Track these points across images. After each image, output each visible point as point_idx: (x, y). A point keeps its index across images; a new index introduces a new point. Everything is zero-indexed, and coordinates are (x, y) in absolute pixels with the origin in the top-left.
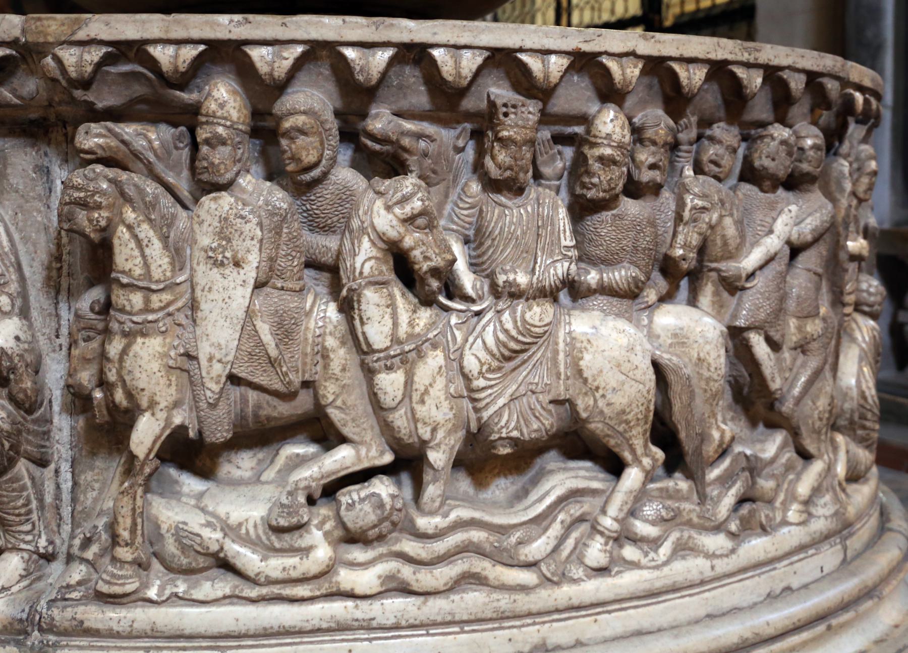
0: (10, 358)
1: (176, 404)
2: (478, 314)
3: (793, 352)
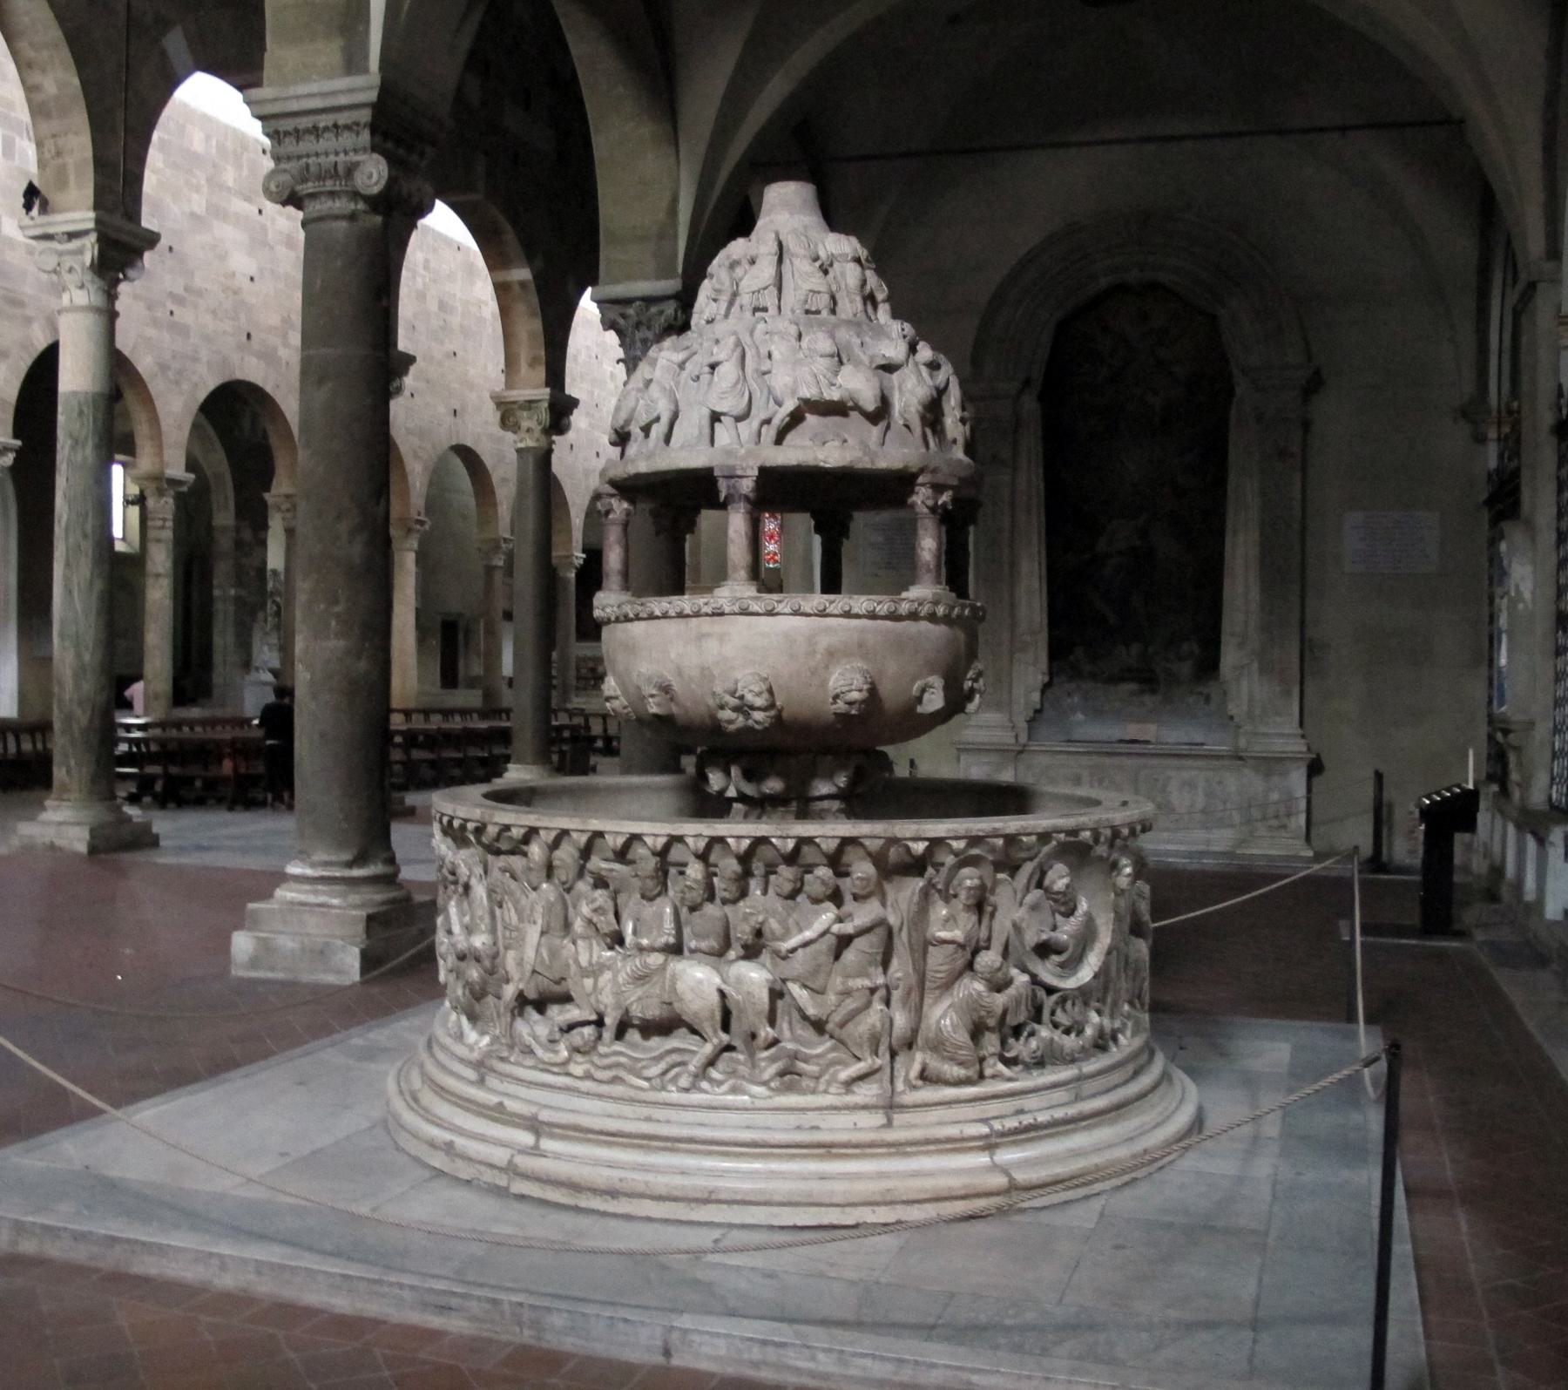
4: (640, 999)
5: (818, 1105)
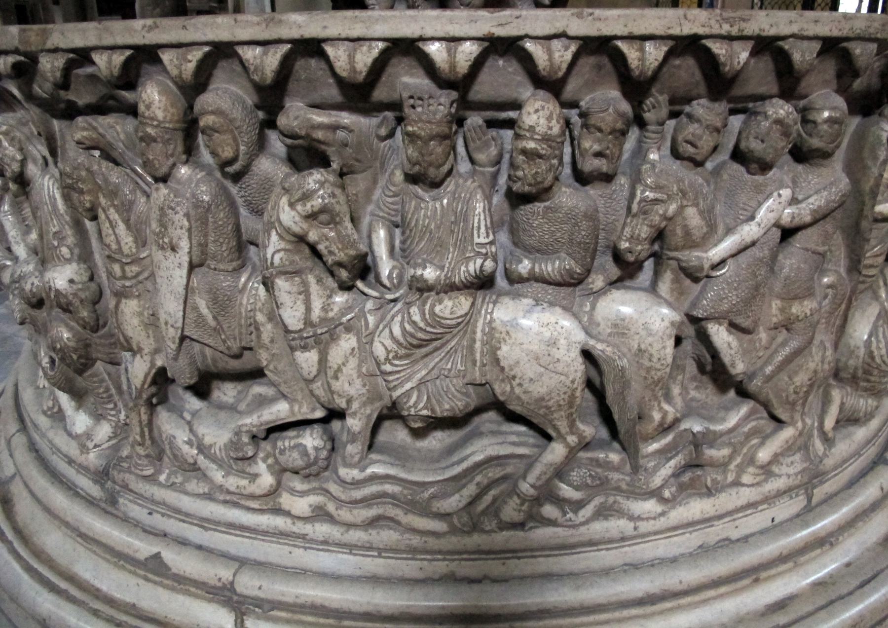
0: (65, 296)
1: (157, 351)
2: (395, 301)
3: (773, 332)
4: (422, 382)
5: (730, 506)
